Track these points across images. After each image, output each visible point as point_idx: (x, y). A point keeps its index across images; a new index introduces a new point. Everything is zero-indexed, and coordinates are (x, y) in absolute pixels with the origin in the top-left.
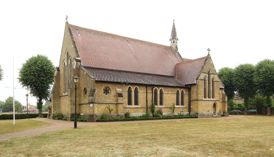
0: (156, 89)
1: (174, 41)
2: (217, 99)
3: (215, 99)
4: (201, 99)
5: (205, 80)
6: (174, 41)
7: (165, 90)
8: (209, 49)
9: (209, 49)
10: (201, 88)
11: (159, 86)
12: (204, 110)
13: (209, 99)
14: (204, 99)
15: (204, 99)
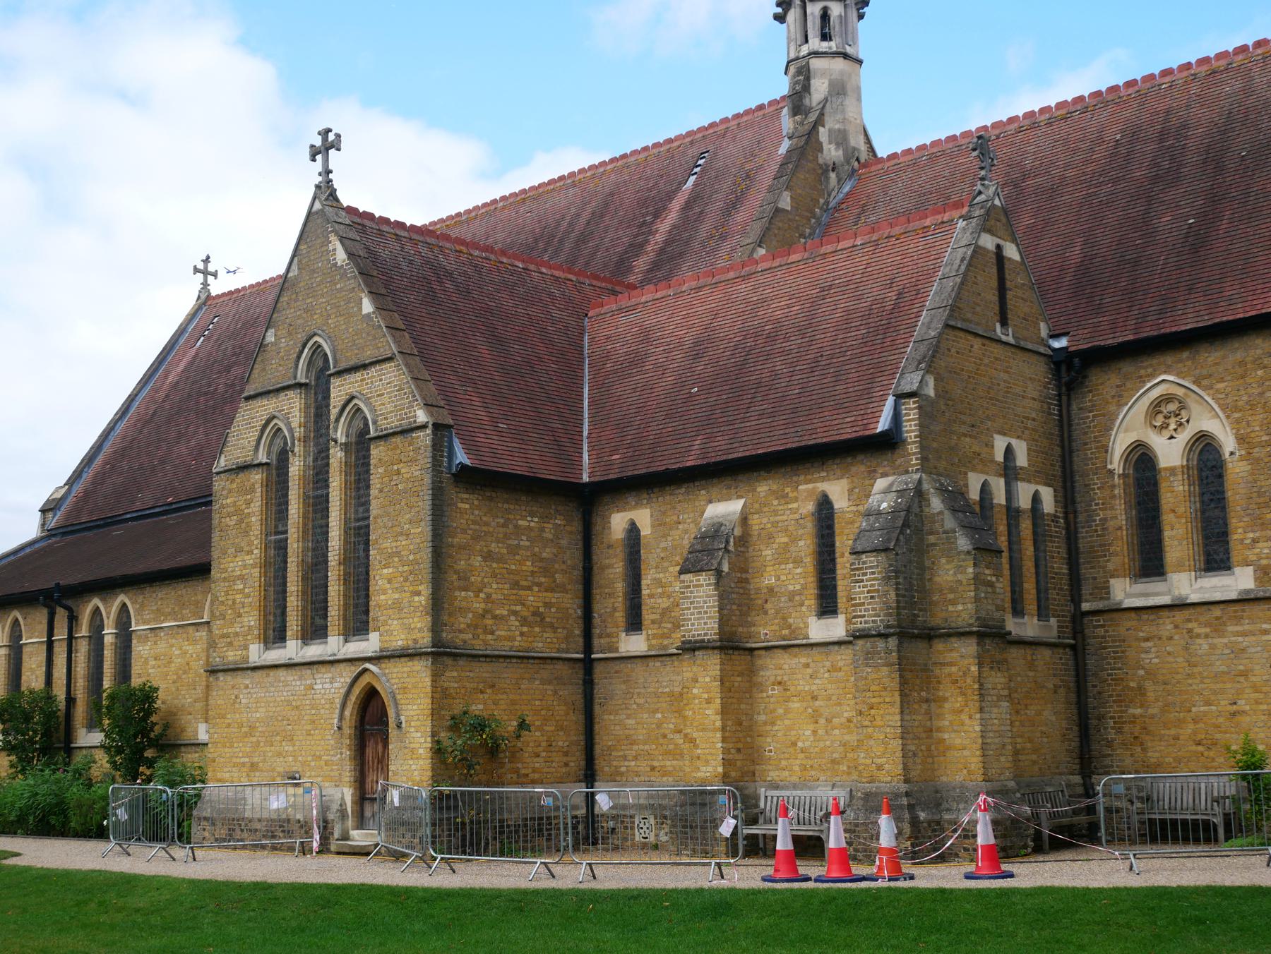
0: (97, 611)
1: (825, 16)
2: (399, 641)
3: (370, 645)
4: (232, 656)
5: (278, 471)
6: (825, 16)
7: (142, 605)
8: (318, 142)
9: (318, 142)
10: (239, 550)
11: (106, 587)
12: (254, 766)
13: (314, 651)
14: (256, 653)
15: (256, 653)
